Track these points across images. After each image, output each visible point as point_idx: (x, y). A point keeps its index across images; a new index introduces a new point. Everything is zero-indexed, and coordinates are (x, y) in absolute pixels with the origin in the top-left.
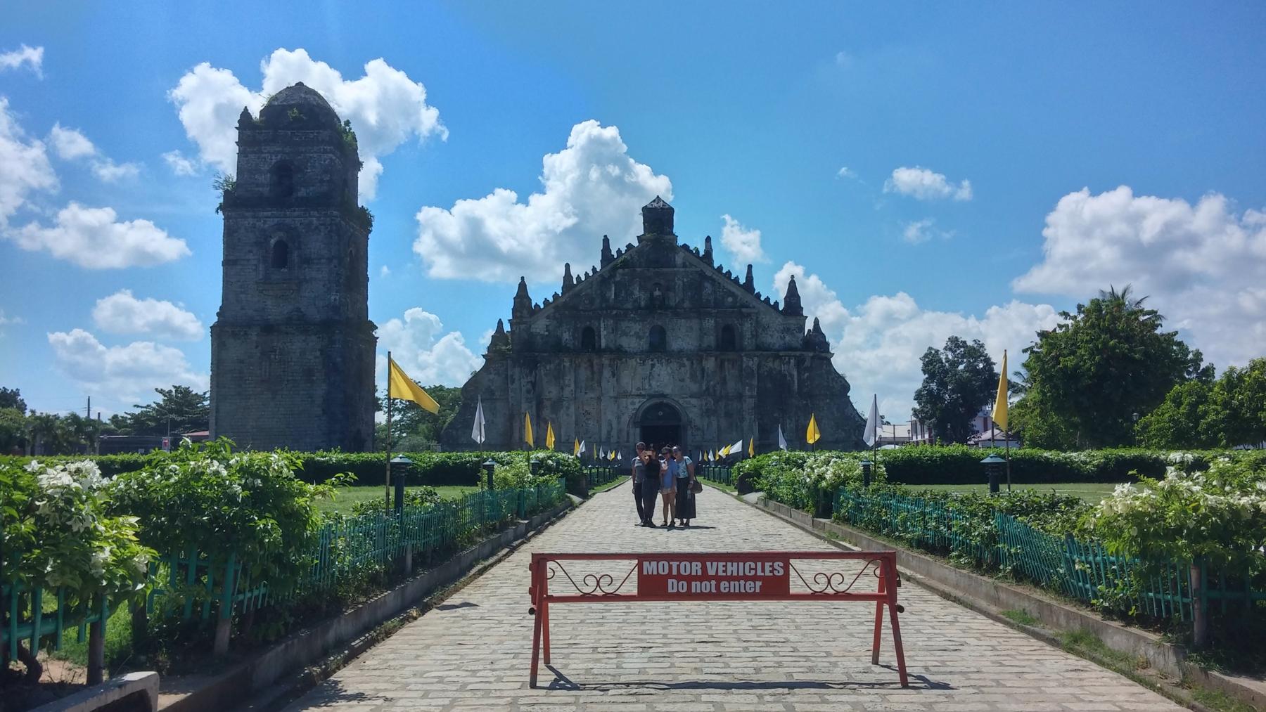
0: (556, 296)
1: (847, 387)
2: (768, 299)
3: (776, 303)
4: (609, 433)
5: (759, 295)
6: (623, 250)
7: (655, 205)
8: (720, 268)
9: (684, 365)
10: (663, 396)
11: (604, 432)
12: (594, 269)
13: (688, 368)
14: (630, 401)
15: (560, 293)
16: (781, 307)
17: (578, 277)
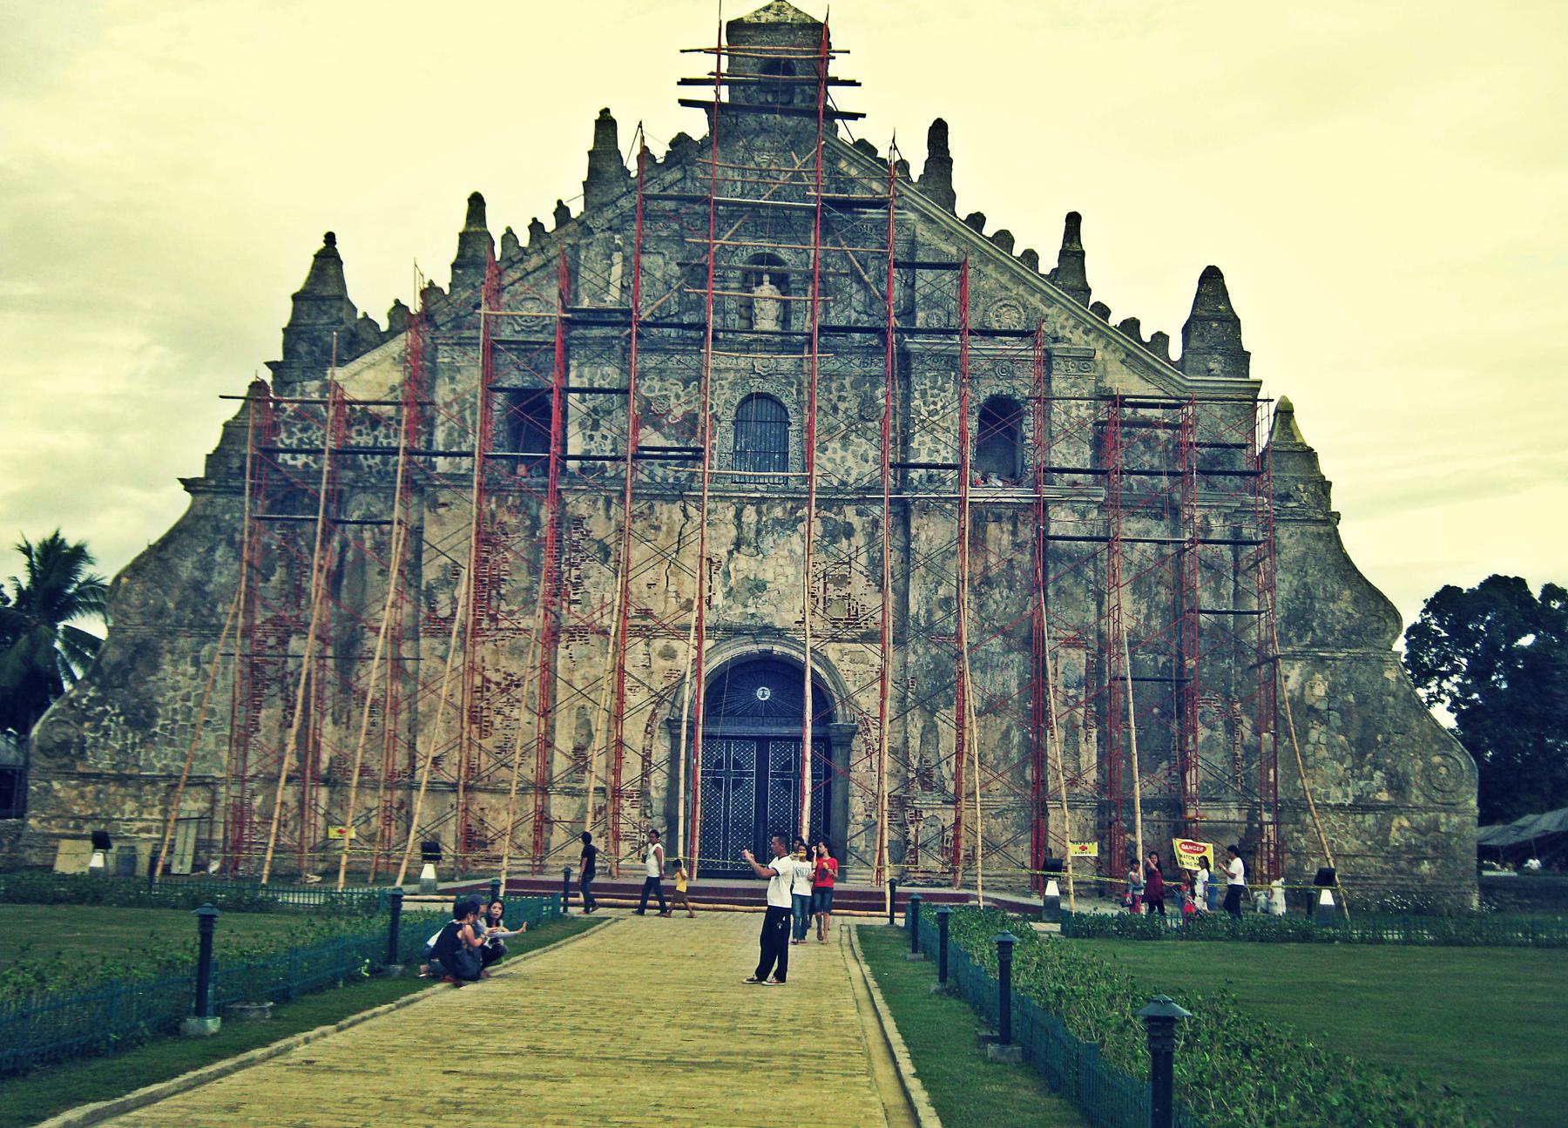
0: (429, 292)
1: (1496, 576)
2: (1131, 326)
3: (1161, 339)
4: (579, 750)
5: (1103, 311)
6: (660, 151)
7: (770, 17)
8: (977, 220)
9: (849, 532)
10: (768, 631)
11: (564, 742)
12: (562, 211)
13: (859, 540)
14: (659, 644)
15: (444, 281)
16: (1175, 351)
17: (509, 235)
